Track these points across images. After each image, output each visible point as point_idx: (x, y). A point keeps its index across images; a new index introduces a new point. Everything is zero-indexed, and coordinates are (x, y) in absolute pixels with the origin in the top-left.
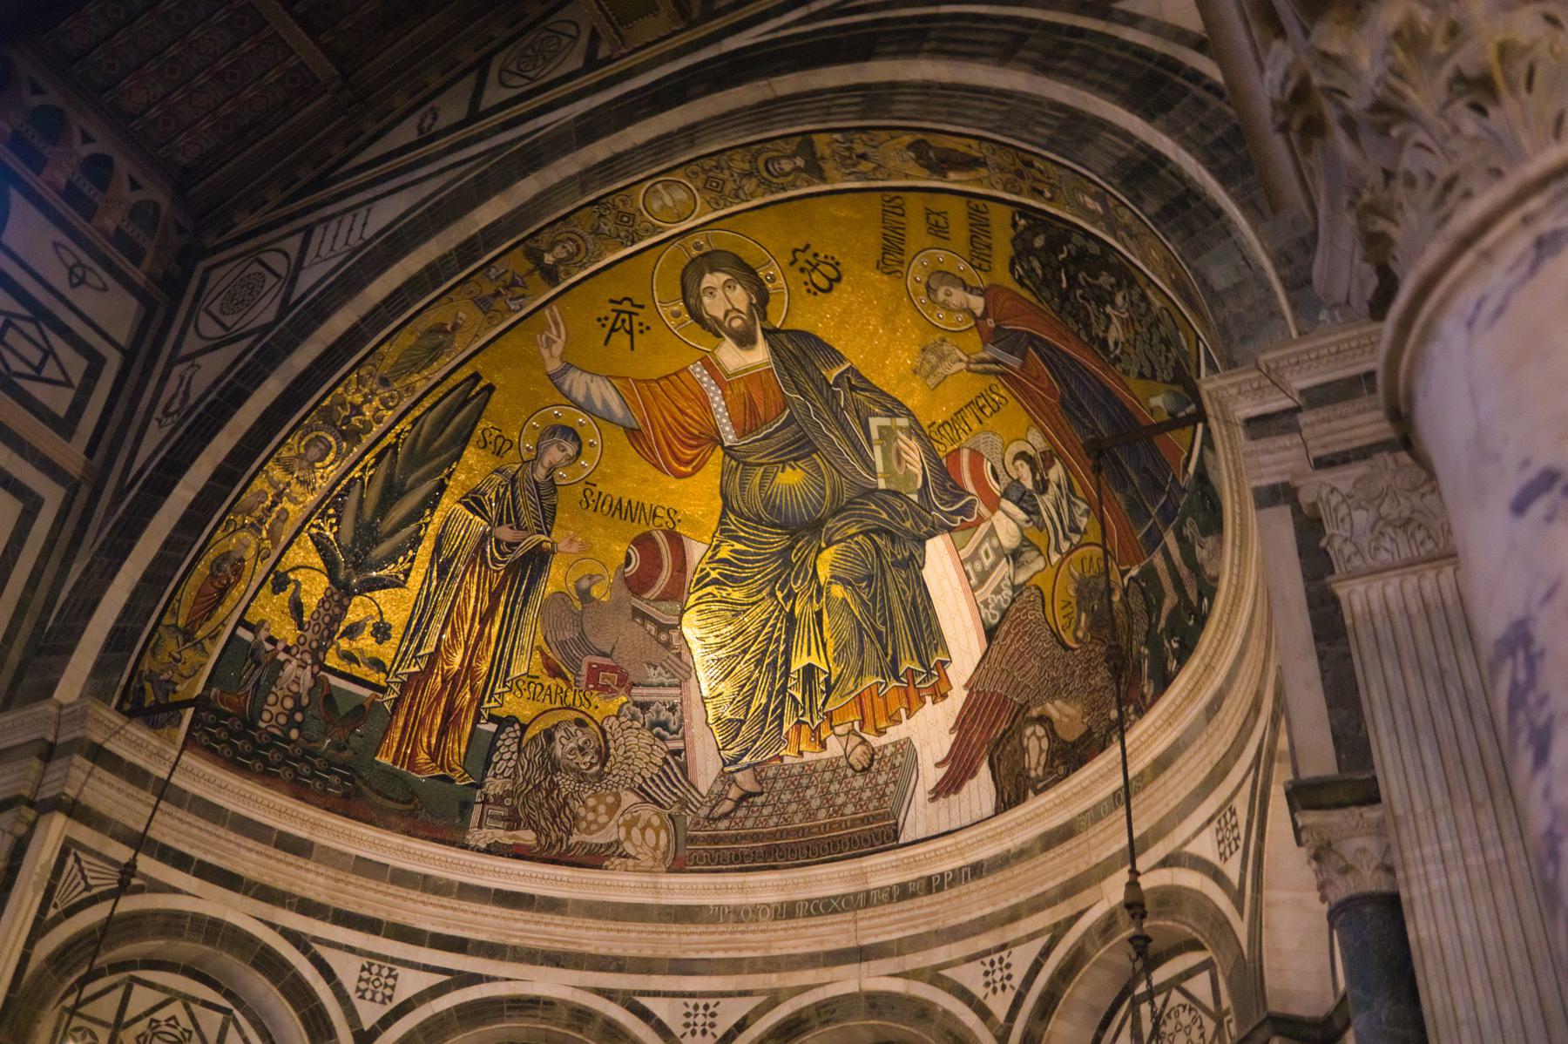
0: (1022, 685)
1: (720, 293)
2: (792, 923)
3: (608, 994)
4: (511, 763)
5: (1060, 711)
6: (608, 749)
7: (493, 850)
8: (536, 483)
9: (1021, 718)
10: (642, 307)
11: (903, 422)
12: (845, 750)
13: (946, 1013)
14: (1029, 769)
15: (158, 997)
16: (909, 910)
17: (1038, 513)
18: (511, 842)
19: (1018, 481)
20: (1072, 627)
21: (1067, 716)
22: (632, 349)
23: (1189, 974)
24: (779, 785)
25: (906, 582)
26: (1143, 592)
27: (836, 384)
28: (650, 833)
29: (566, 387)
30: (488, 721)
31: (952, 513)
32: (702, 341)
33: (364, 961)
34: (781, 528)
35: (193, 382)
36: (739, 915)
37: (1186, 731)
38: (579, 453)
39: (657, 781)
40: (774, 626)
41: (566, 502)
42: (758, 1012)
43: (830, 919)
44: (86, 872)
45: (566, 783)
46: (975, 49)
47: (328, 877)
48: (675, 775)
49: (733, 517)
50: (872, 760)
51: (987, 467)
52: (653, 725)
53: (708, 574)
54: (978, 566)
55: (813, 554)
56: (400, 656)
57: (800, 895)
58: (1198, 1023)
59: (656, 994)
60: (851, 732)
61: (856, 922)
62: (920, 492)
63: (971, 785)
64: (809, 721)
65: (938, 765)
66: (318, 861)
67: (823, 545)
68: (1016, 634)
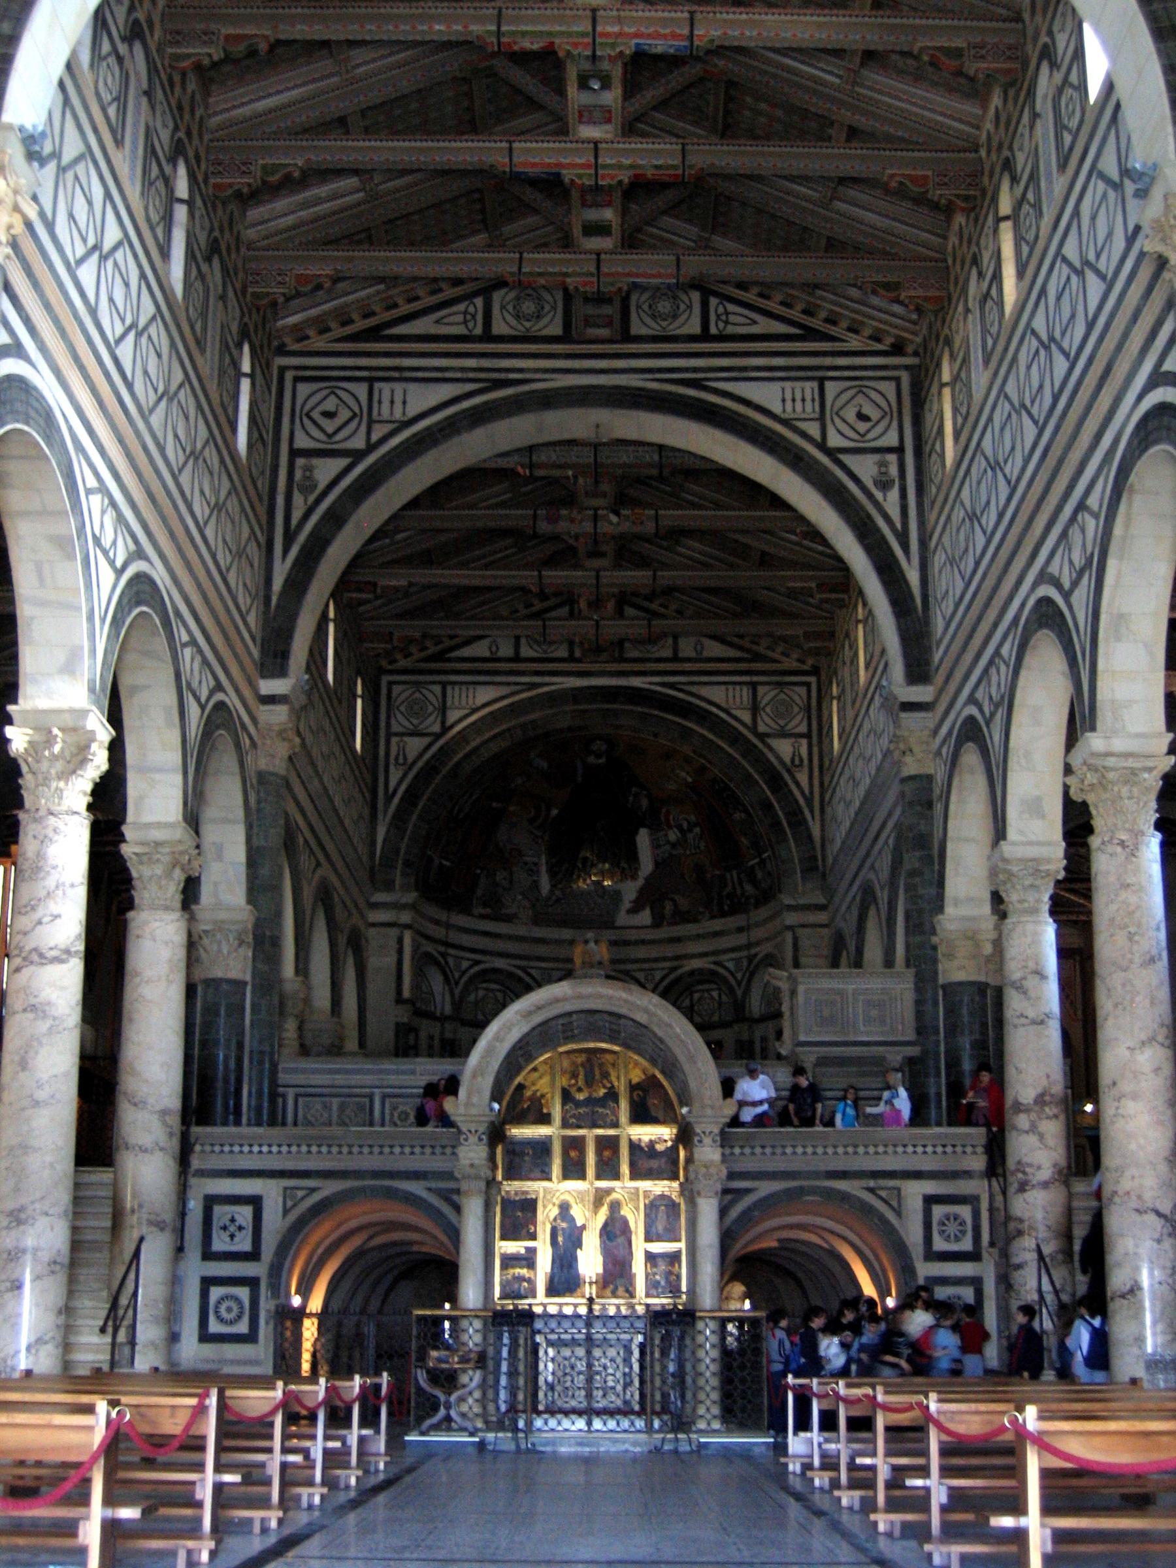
3: (518, 967)
7: (483, 917)
35: (407, 750)
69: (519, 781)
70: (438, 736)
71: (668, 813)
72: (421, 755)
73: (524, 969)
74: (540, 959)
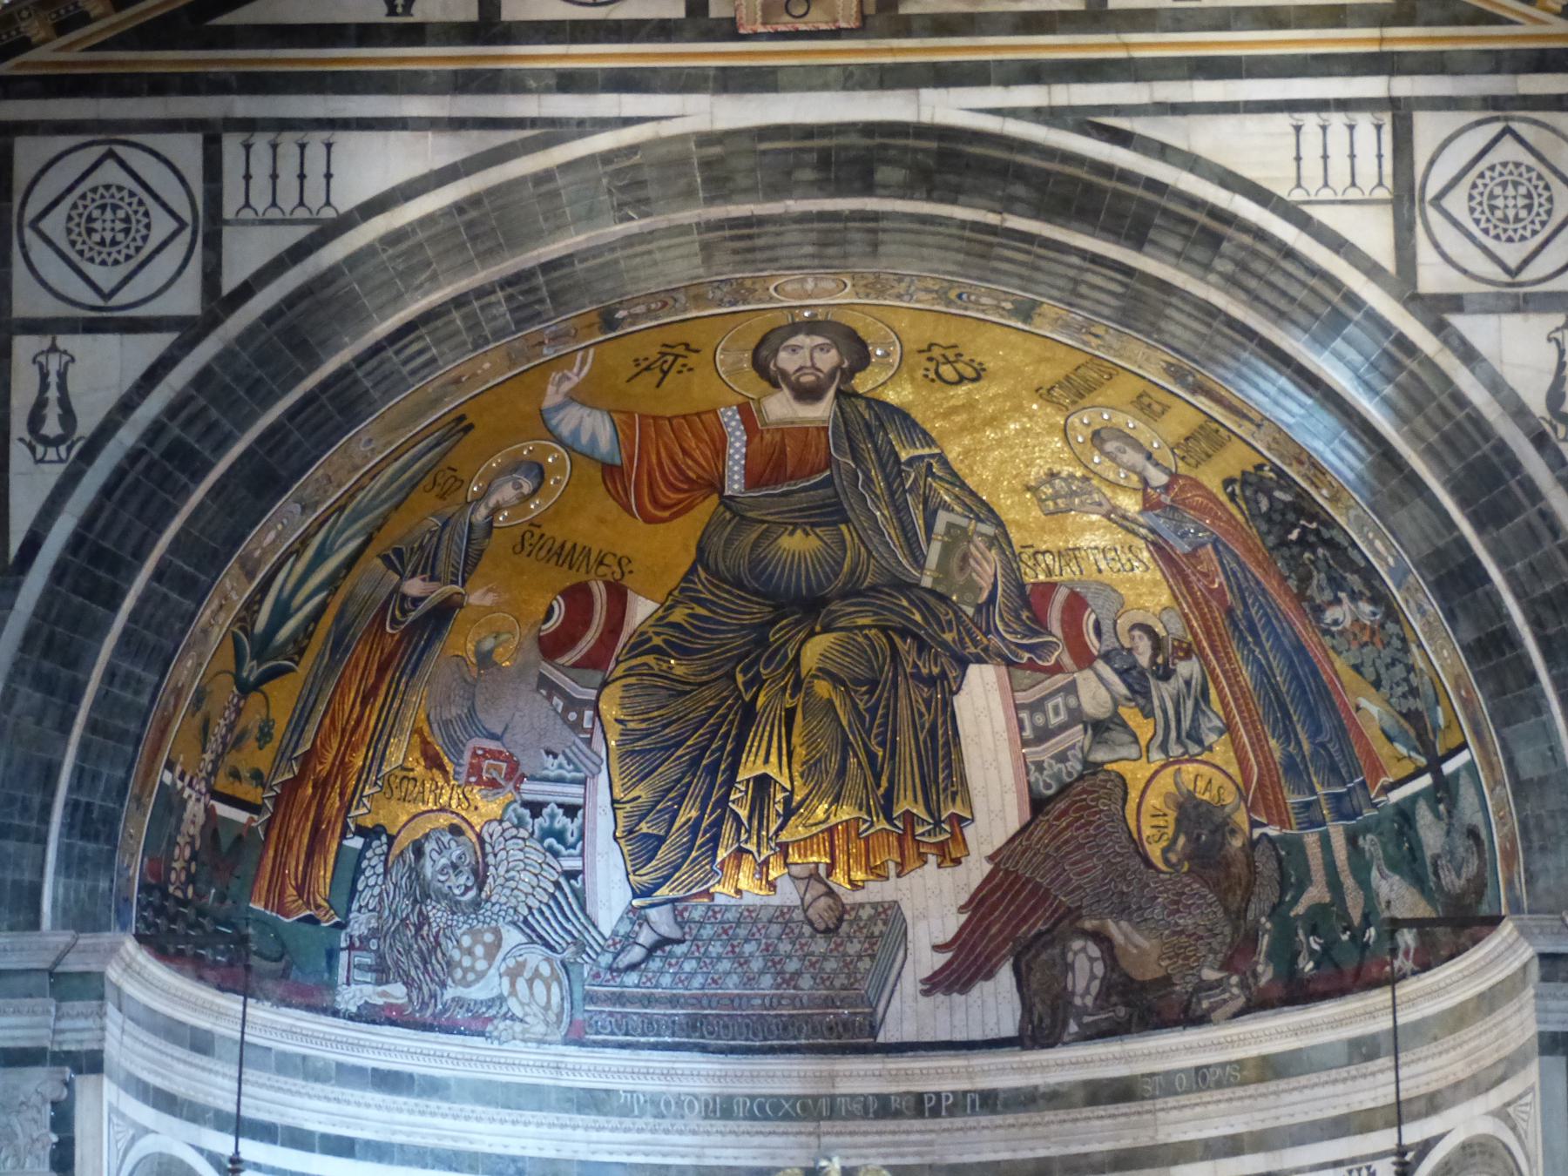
0: (1075, 883)
1: (807, 352)
2: (731, 1125)
4: (377, 891)
5: (1126, 936)
6: (487, 865)
7: (368, 1015)
8: (471, 524)
9: (1066, 922)
10: (697, 351)
11: (988, 529)
12: (802, 900)
14: (1073, 993)
17: (1146, 695)
18: (380, 1001)
19: (1130, 650)
20: (1164, 844)
21: (1136, 947)
22: (658, 385)
24: (707, 932)
25: (928, 703)
26: (1280, 860)
27: (911, 461)
28: (539, 987)
29: (554, 422)
30: (355, 834)
31: (1017, 645)
32: (751, 385)
34: (764, 596)
35: (72, 387)
37: (1313, 1048)
38: (534, 492)
39: (548, 913)
40: (725, 716)
41: (497, 543)
43: (783, 1126)
45: (437, 914)
46: (1282, 304)
48: (570, 905)
49: (703, 575)
50: (840, 920)
51: (1089, 621)
52: (549, 832)
53: (650, 639)
54: (1039, 720)
55: (802, 635)
56: (282, 755)
60: (813, 876)
61: (819, 1136)
62: (979, 608)
63: (982, 989)
64: (754, 849)
65: (937, 948)
66: (220, 1058)
67: (818, 628)
68: (1078, 819)
69: (506, 493)
70: (191, 331)
71: (1076, 604)
72: (126, 406)
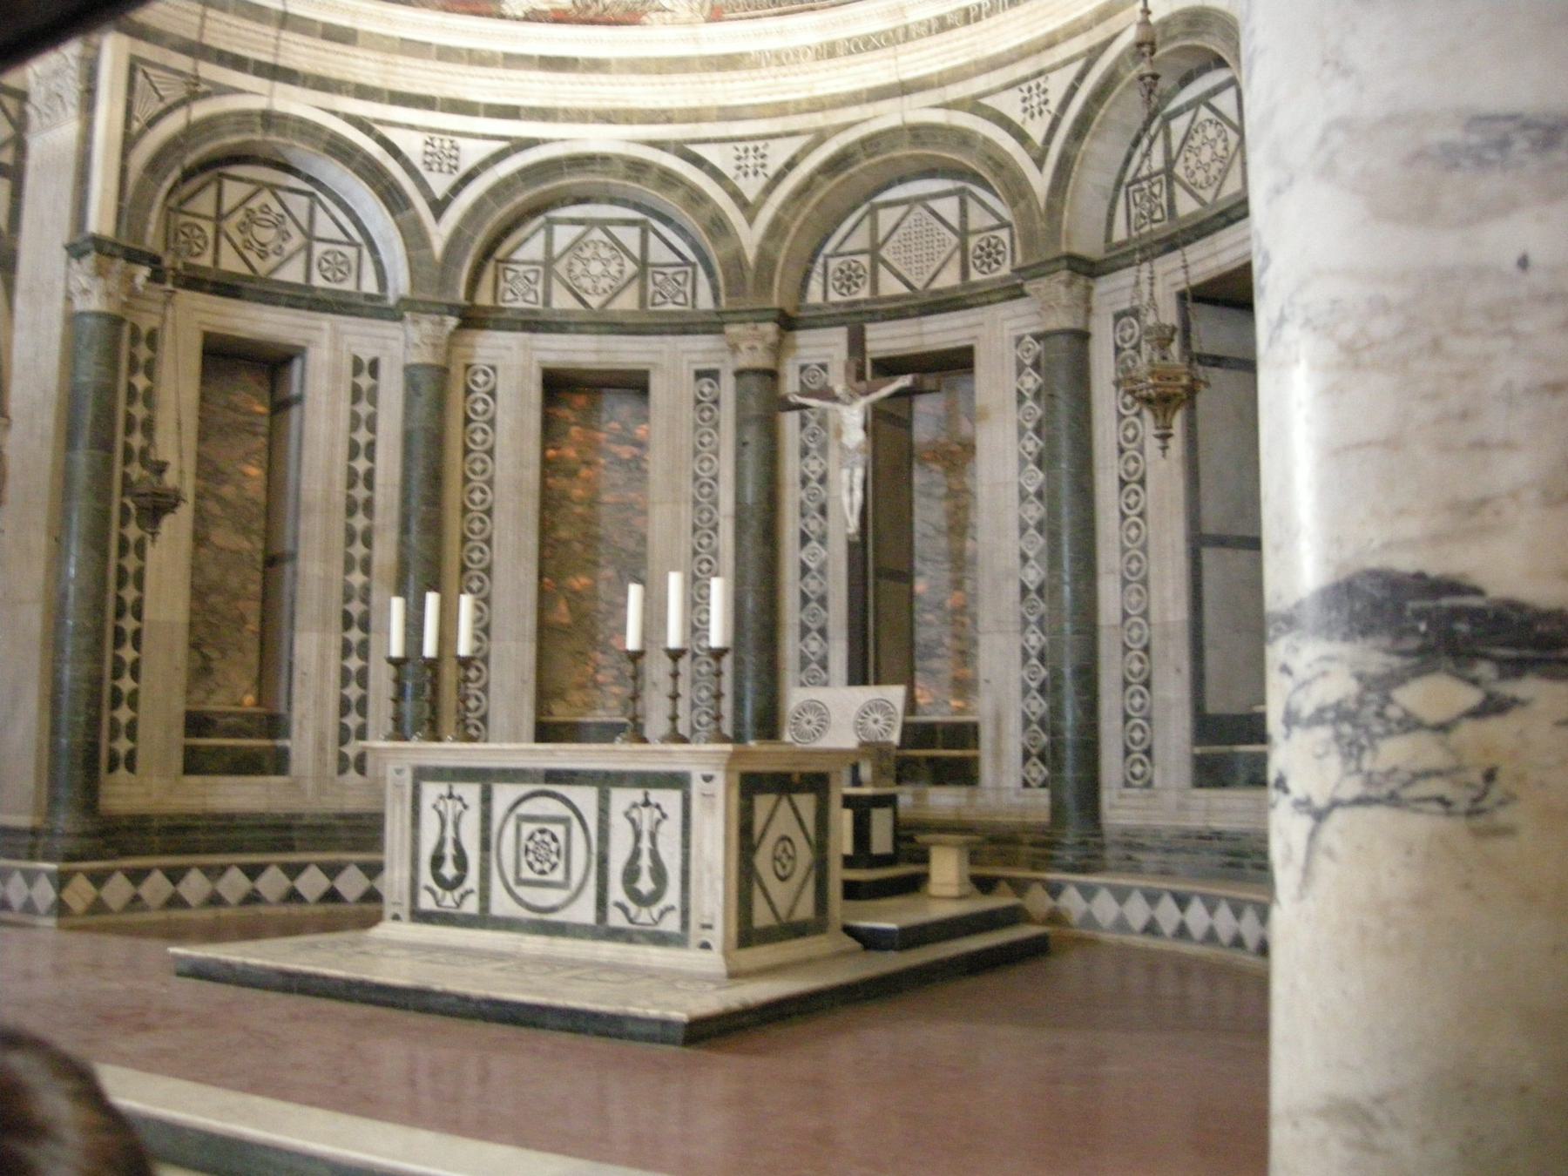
2: (833, 62)
13: (987, 141)
15: (247, 189)
16: (948, 42)
23: (1216, 91)
33: (426, 136)
36: (779, 58)
42: (806, 151)
44: (157, 85)
47: (377, 61)
57: (839, 35)
58: (1223, 136)
59: (706, 141)
61: (896, 58)
73: (682, 150)
74: (729, 114)
